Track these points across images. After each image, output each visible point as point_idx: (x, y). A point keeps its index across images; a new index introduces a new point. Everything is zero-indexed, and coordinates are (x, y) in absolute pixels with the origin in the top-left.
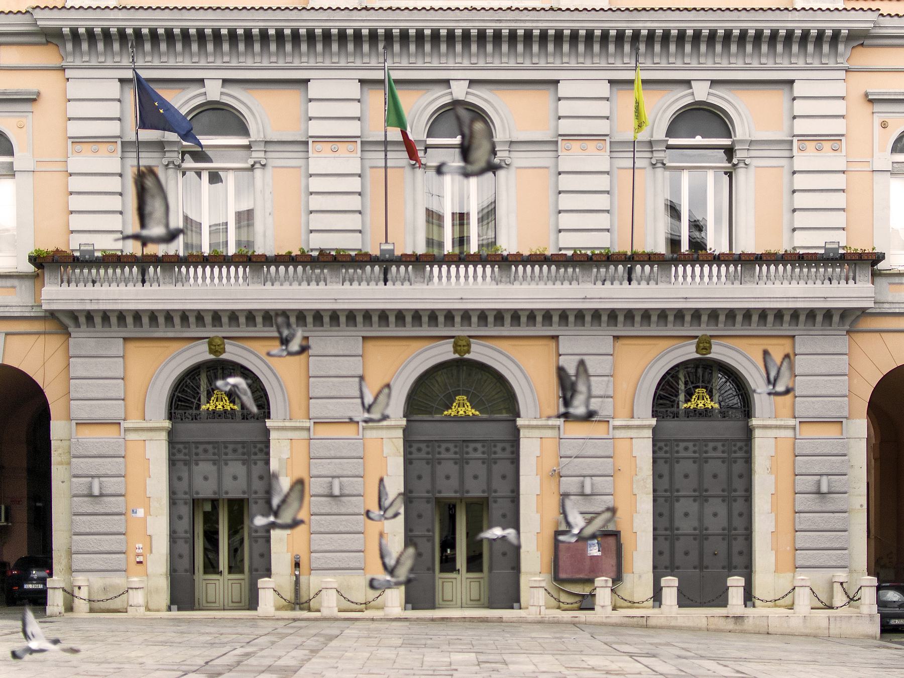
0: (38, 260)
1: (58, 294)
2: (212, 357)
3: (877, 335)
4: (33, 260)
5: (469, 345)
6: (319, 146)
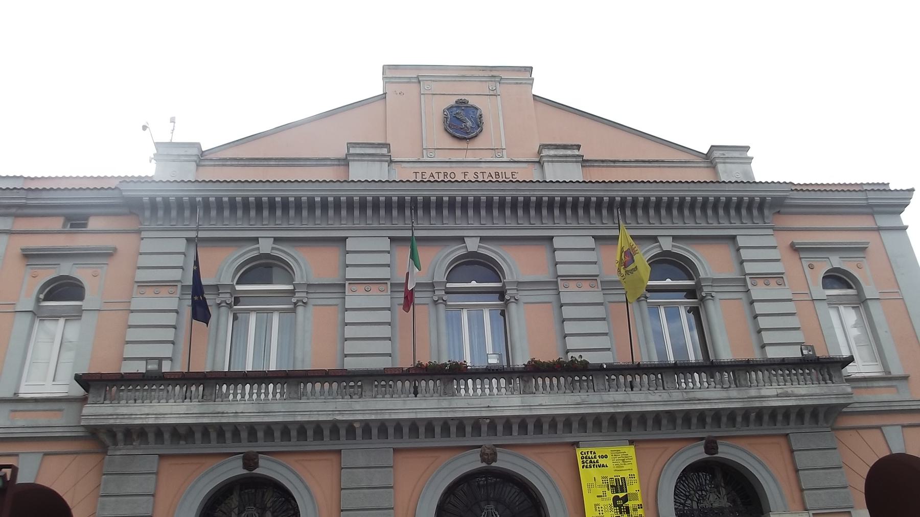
0: (84, 380)
2: (245, 472)
3: (853, 432)
5: (495, 454)
6: (354, 287)
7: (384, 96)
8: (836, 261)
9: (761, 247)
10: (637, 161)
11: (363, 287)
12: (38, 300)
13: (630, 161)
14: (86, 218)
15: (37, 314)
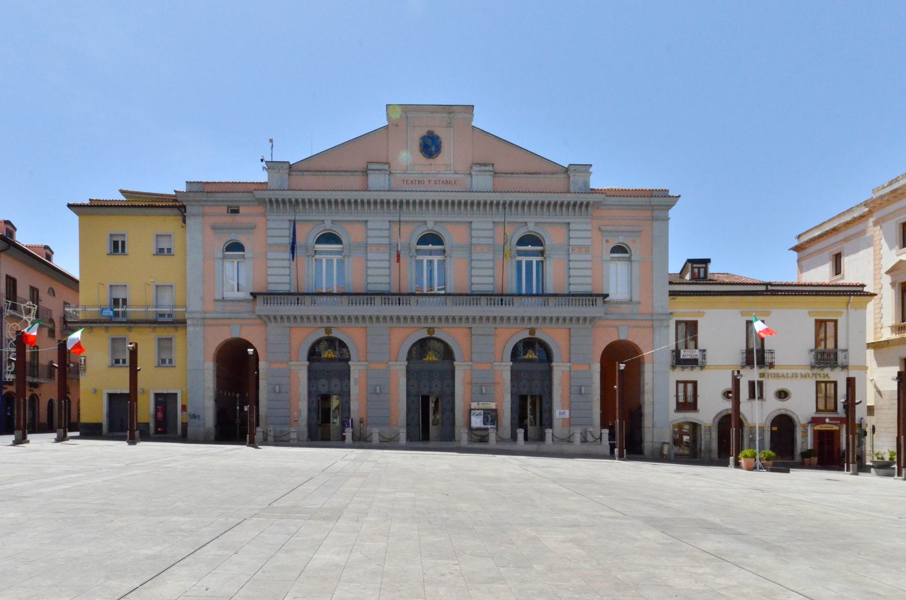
0: (254, 295)
1: (262, 308)
4: (251, 294)
7: (386, 127)
9: (582, 229)
15: (224, 257)
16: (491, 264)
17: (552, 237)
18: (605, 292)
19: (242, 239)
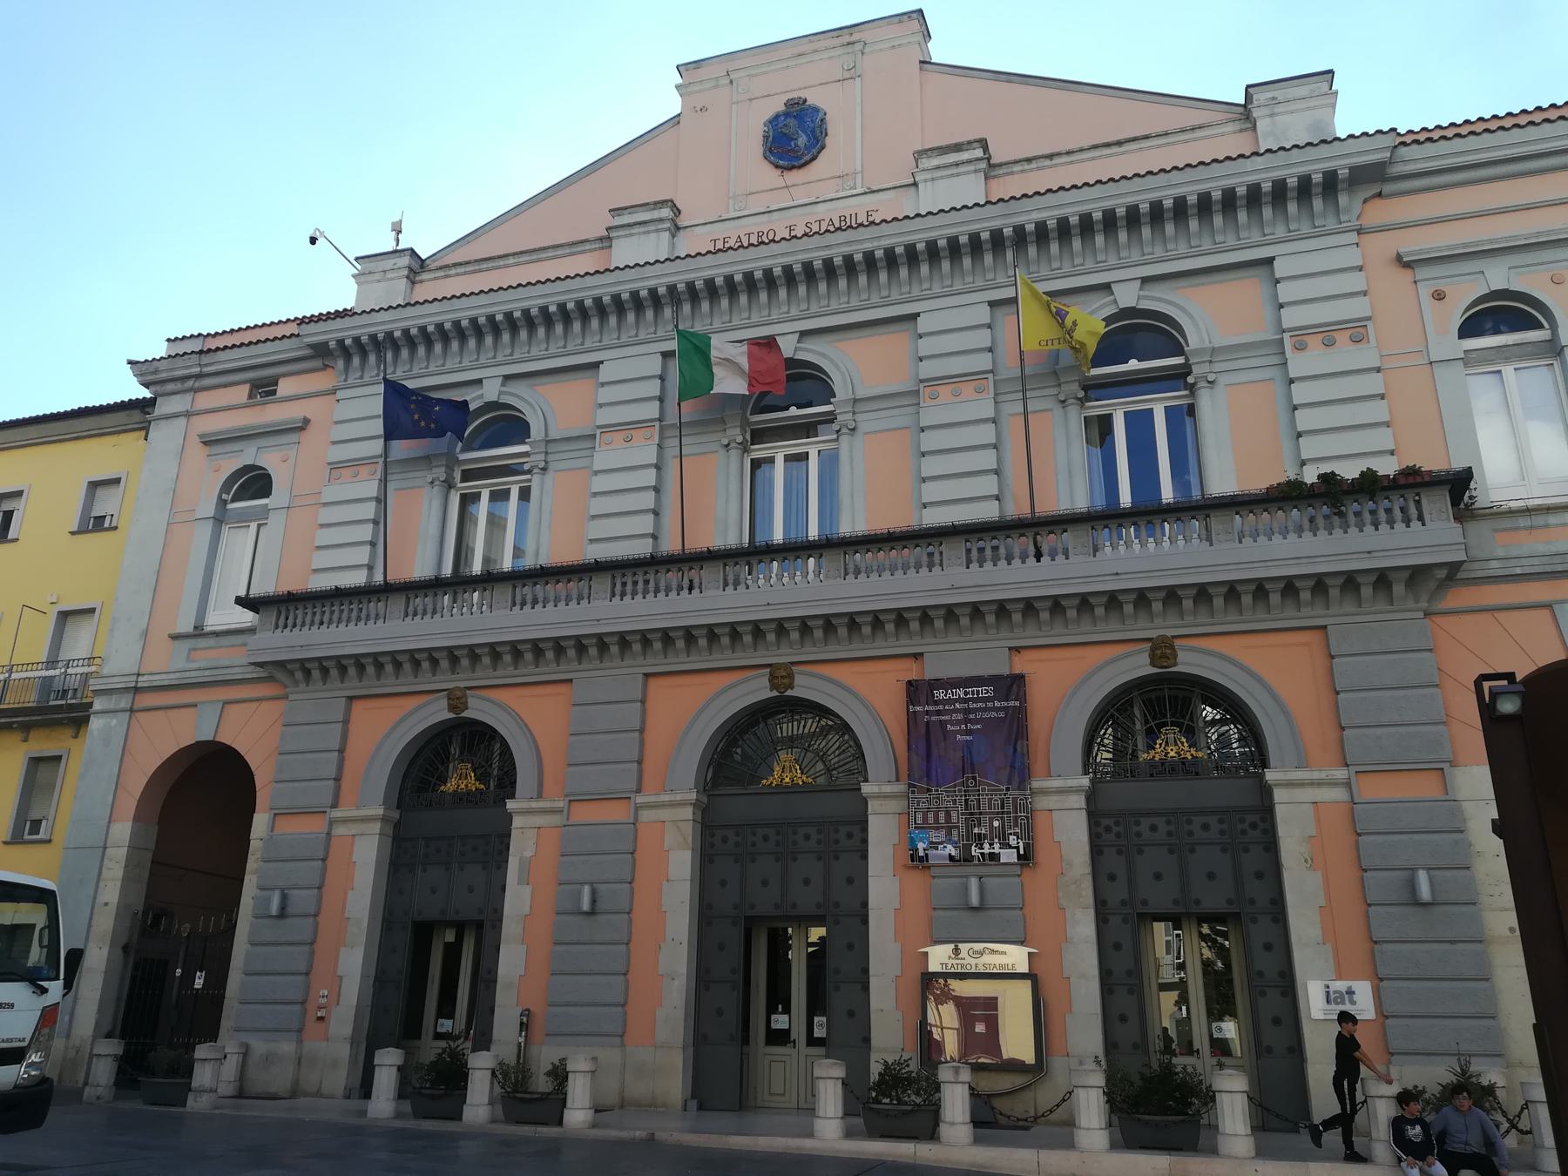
2: (452, 715)
3: (1487, 616)
5: (791, 676)
6: (607, 437)
8: (1498, 276)
9: (1319, 267)
10: (1095, 147)
11: (621, 435)
12: (222, 503)
13: (1081, 150)
14: (274, 382)
16: (987, 434)
17: (1208, 317)
18: (1458, 464)
19: (270, 459)
